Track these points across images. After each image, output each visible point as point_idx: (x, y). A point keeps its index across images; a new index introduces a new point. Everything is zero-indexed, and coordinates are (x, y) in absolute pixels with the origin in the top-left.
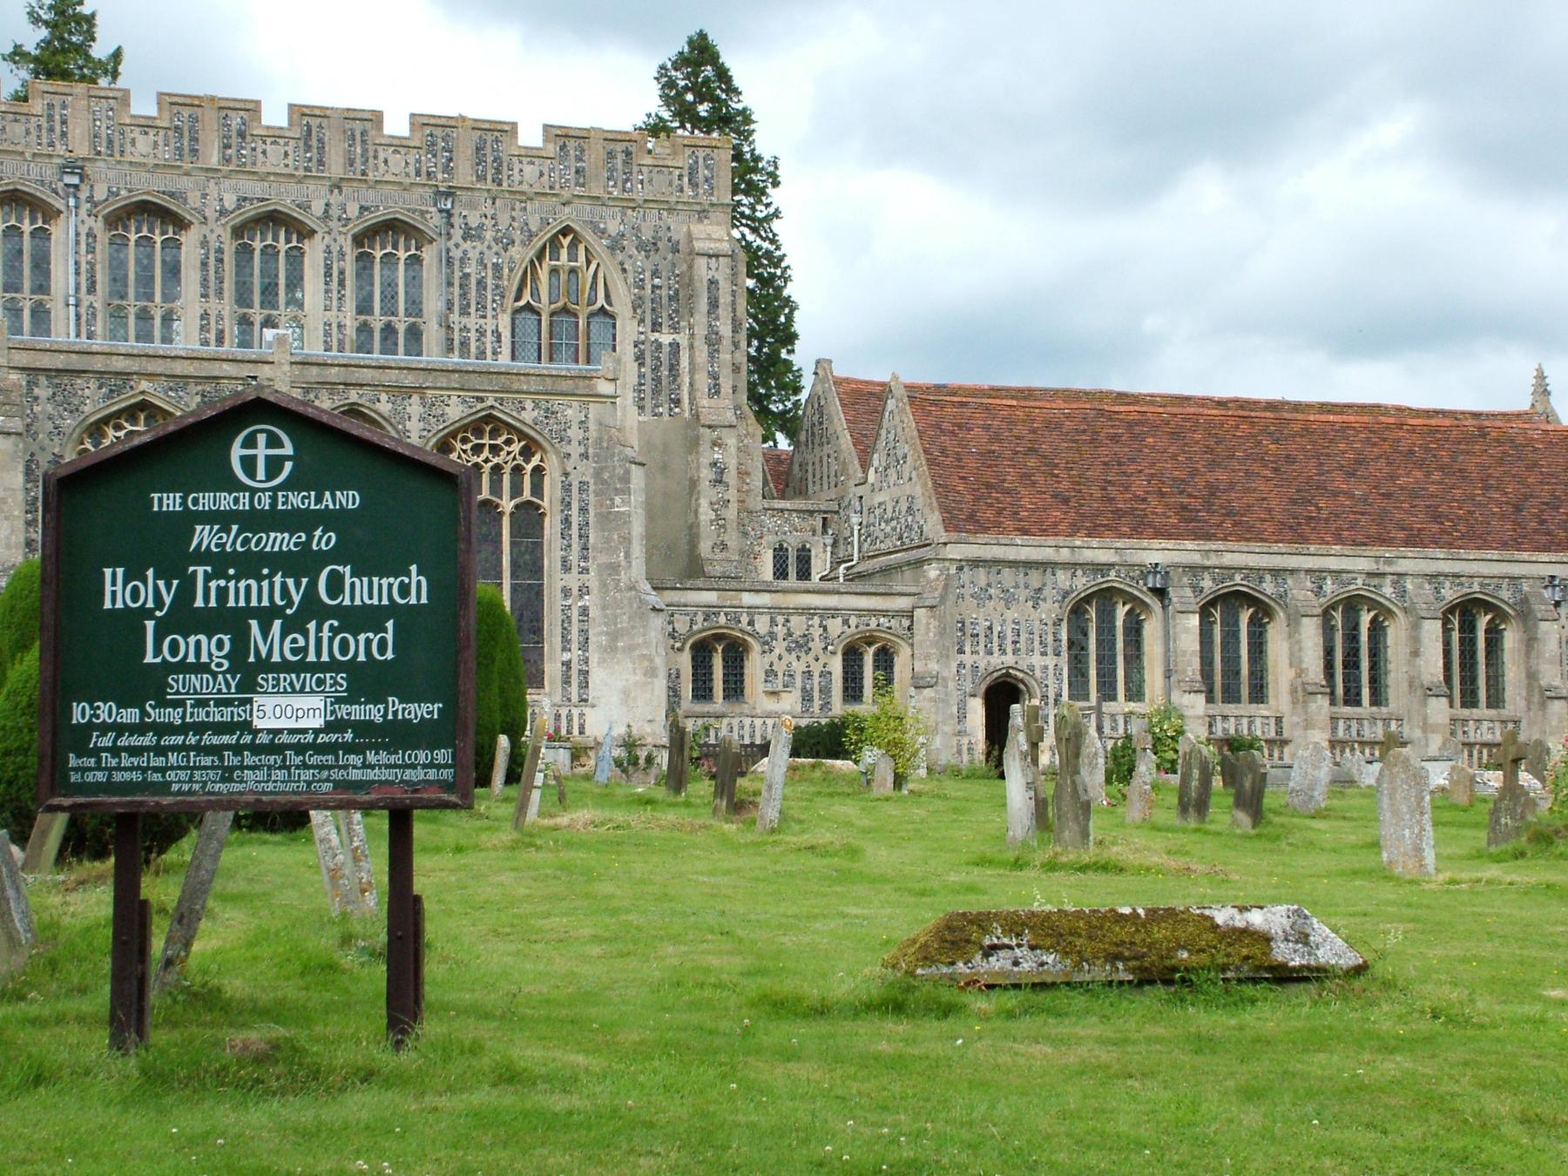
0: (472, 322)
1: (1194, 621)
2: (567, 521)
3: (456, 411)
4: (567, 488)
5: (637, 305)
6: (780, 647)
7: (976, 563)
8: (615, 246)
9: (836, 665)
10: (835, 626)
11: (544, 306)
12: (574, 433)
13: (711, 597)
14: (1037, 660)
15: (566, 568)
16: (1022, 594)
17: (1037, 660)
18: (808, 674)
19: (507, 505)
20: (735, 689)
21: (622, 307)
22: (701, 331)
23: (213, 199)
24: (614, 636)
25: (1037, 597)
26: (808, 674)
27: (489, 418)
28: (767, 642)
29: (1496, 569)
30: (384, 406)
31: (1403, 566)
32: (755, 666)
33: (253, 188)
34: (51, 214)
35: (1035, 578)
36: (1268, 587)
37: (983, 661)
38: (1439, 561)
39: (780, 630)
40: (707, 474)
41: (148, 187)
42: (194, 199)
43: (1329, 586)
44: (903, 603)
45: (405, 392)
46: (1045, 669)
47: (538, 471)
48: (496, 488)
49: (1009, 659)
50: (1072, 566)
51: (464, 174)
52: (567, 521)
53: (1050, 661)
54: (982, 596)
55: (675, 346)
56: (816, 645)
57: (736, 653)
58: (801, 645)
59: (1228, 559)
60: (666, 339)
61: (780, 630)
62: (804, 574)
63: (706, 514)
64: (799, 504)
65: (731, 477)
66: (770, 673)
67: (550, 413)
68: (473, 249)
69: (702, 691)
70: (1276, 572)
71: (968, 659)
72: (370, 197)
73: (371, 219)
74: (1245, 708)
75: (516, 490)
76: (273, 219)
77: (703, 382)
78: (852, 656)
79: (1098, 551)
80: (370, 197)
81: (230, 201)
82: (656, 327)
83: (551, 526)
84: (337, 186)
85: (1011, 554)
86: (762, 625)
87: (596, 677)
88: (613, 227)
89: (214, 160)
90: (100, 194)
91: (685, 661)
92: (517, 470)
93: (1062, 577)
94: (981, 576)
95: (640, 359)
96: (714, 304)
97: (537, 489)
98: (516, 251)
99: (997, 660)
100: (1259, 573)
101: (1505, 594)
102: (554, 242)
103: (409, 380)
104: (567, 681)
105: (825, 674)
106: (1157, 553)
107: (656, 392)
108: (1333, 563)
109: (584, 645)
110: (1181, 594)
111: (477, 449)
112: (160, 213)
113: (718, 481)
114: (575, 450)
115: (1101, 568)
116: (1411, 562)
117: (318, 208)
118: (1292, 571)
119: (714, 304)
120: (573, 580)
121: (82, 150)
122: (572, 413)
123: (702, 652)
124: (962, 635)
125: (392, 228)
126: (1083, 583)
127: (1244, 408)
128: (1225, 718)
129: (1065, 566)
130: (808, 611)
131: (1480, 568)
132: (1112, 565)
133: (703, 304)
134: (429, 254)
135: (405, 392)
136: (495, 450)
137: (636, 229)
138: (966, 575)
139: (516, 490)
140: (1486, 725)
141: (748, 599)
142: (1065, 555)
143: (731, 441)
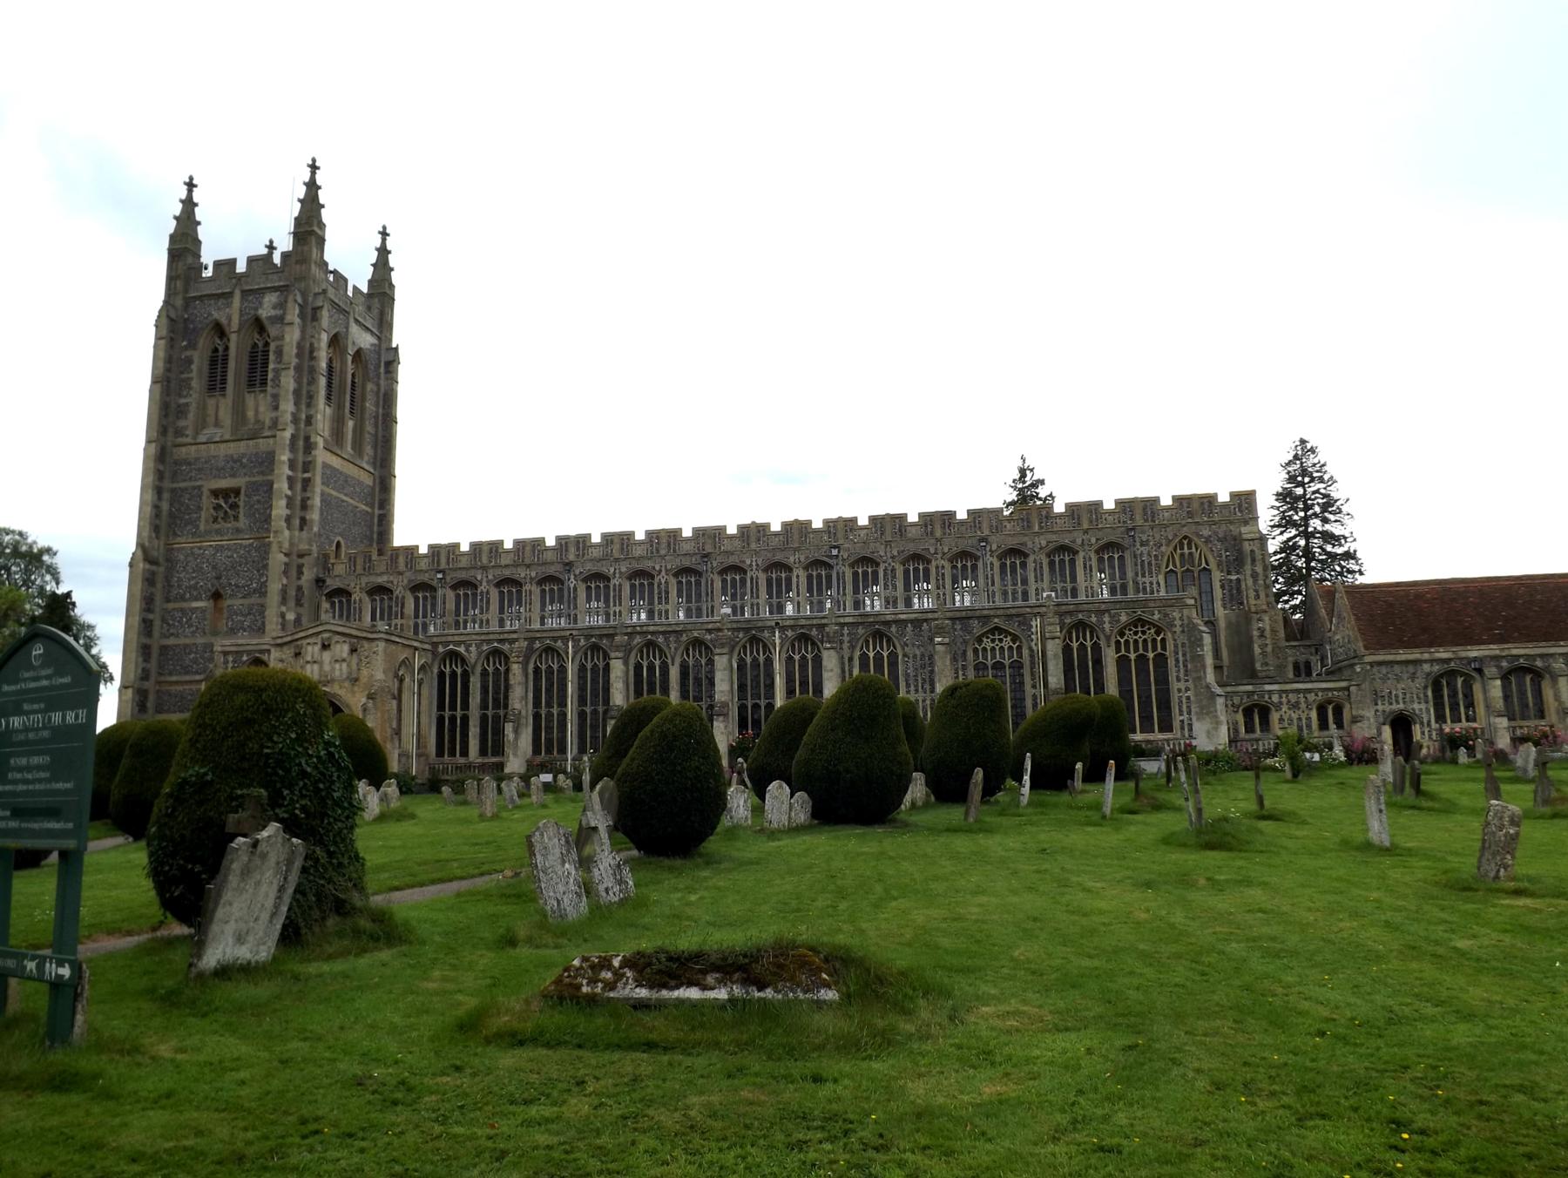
0: (1147, 580)
1: (1498, 682)
2: (1177, 660)
3: (1124, 618)
4: (1176, 646)
5: (1219, 565)
6: (1285, 708)
7: (1380, 664)
8: (1208, 540)
9: (1314, 714)
10: (1311, 697)
11: (1179, 570)
12: (1178, 622)
13: (1250, 688)
14: (1416, 706)
15: (1178, 680)
16: (1405, 676)
18: (1300, 719)
19: (1132, 656)
21: (1213, 566)
22: (1249, 572)
24: (1202, 708)
25: (1413, 677)
26: (1300, 719)
27: (1140, 620)
28: (1278, 708)
30: (1094, 619)
32: (1275, 717)
33: (1054, 537)
34: (977, 558)
35: (1411, 668)
36: (1539, 663)
37: (1388, 708)
39: (1284, 700)
40: (1256, 633)
41: (1012, 542)
42: (1030, 544)
44: (1344, 684)
45: (1100, 613)
46: (1422, 709)
47: (1163, 640)
48: (1145, 649)
49: (1401, 706)
50: (1432, 661)
51: (1139, 521)
52: (1177, 660)
53: (1423, 706)
54: (1384, 679)
55: (1238, 580)
56: (1303, 706)
57: (1265, 712)
58: (1295, 706)
59: (1515, 652)
60: (1234, 577)
61: (1284, 700)
62: (1309, 674)
63: (1257, 650)
64: (1308, 643)
65: (1268, 633)
66: (1281, 720)
67: (1166, 615)
69: (1250, 728)
70: (1542, 656)
71: (1380, 707)
72: (1100, 534)
73: (1101, 543)
74: (1532, 723)
75: (1154, 649)
76: (1063, 548)
77: (1252, 594)
78: (1322, 710)
79: (1443, 654)
80: (1100, 534)
81: (1044, 543)
82: (1229, 573)
83: (1171, 662)
84: (1086, 532)
85: (1399, 658)
86: (1275, 698)
87: (1197, 726)
88: (1206, 532)
89: (1036, 528)
90: (994, 547)
91: (1240, 718)
92: (1154, 640)
94: (1384, 670)
95: (1222, 587)
96: (1253, 560)
97: (1164, 648)
98: (1163, 548)
99: (1395, 707)
100: (1533, 657)
102: (1181, 543)
103: (1103, 607)
104: (1182, 728)
105: (1309, 719)
106: (1474, 652)
107: (1231, 600)
109: (1189, 713)
110: (1490, 671)
111: (1136, 633)
112: (1017, 552)
113: (1262, 636)
114: (1178, 629)
115: (1447, 661)
117: (1079, 541)
119: (1253, 560)
120: (1182, 685)
121: (986, 532)
122: (1176, 615)
123: (1248, 712)
124: (1377, 697)
125: (1110, 546)
126: (1436, 668)
129: (1426, 661)
130: (1298, 691)
132: (1451, 659)
133: (1249, 561)
134: (1127, 555)
135: (1100, 613)
136: (1144, 633)
137: (1216, 533)
138: (1375, 669)
139: (1154, 649)
141: (1267, 687)
142: (1426, 656)
143: (1266, 618)
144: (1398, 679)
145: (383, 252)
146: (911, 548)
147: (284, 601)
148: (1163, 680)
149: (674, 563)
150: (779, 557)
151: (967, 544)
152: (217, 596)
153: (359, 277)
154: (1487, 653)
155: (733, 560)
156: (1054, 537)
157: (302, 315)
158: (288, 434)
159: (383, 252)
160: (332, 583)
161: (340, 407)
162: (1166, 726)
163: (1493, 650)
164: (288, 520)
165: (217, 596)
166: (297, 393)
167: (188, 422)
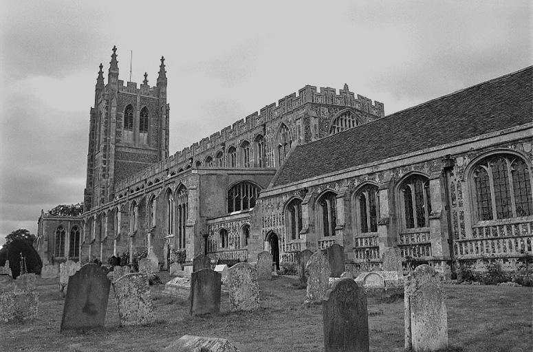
7: (265, 198)
16: (275, 206)
17: (279, 227)
43: (356, 184)
49: (272, 228)
53: (281, 227)
93: (285, 199)
94: (267, 202)
102: (282, 127)
105: (239, 238)
108: (357, 173)
115: (292, 192)
118: (343, 180)
128: (327, 242)
131: (410, 160)
140: (421, 235)
144: (273, 208)
145: (162, 66)
154: (310, 184)
158: (102, 146)
159: (162, 66)
161: (135, 129)
164: (104, 176)
166: (106, 131)
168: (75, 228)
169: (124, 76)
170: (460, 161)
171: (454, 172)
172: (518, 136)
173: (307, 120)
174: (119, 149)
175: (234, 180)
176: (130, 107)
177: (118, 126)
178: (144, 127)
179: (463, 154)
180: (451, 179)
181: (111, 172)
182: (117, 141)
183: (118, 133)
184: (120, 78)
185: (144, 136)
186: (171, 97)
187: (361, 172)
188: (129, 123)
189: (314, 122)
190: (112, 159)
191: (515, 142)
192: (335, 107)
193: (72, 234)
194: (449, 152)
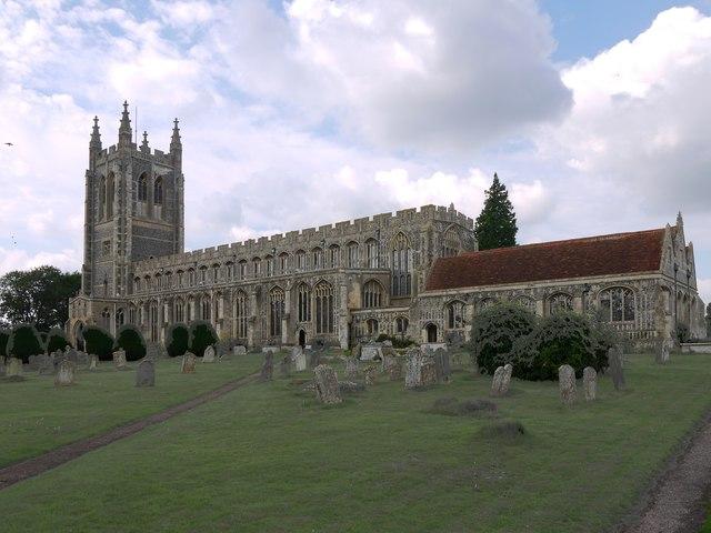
9: (395, 323)
20: (376, 328)
23: (342, 240)
29: (567, 283)
31: (537, 286)
33: (348, 237)
38: (549, 283)
45: (309, 277)
50: (447, 296)
58: (387, 320)
68: (383, 240)
70: (499, 292)
76: (352, 242)
78: (399, 320)
94: (426, 300)
101: (570, 290)
106: (466, 290)
108: (515, 288)
115: (454, 296)
116: (539, 285)
123: (369, 322)
127: (573, 243)
130: (388, 312)
146: (299, 246)
147: (119, 283)
148: (331, 309)
149: (225, 259)
150: (256, 254)
151: (318, 243)
152: (106, 282)
153: (160, 143)
155: (243, 257)
156: (348, 237)
157: (121, 169)
158: (116, 219)
160: (136, 275)
161: (150, 203)
162: (331, 331)
163: (476, 289)
165: (106, 282)
167: (97, 217)
168: (120, 310)
169: (137, 140)
170: (594, 288)
171: (589, 293)
172: (631, 278)
173: (430, 233)
174: (135, 223)
175: (367, 277)
176: (142, 177)
177: (134, 198)
178: (159, 199)
179: (597, 284)
180: (587, 298)
181: (128, 249)
182: (133, 214)
183: (134, 205)
184: (133, 141)
185: (157, 209)
186: (188, 167)
187: (520, 287)
188: (143, 195)
189: (436, 235)
190: (129, 234)
191: (629, 281)
192: (446, 223)
193: (117, 317)
194: (588, 282)
